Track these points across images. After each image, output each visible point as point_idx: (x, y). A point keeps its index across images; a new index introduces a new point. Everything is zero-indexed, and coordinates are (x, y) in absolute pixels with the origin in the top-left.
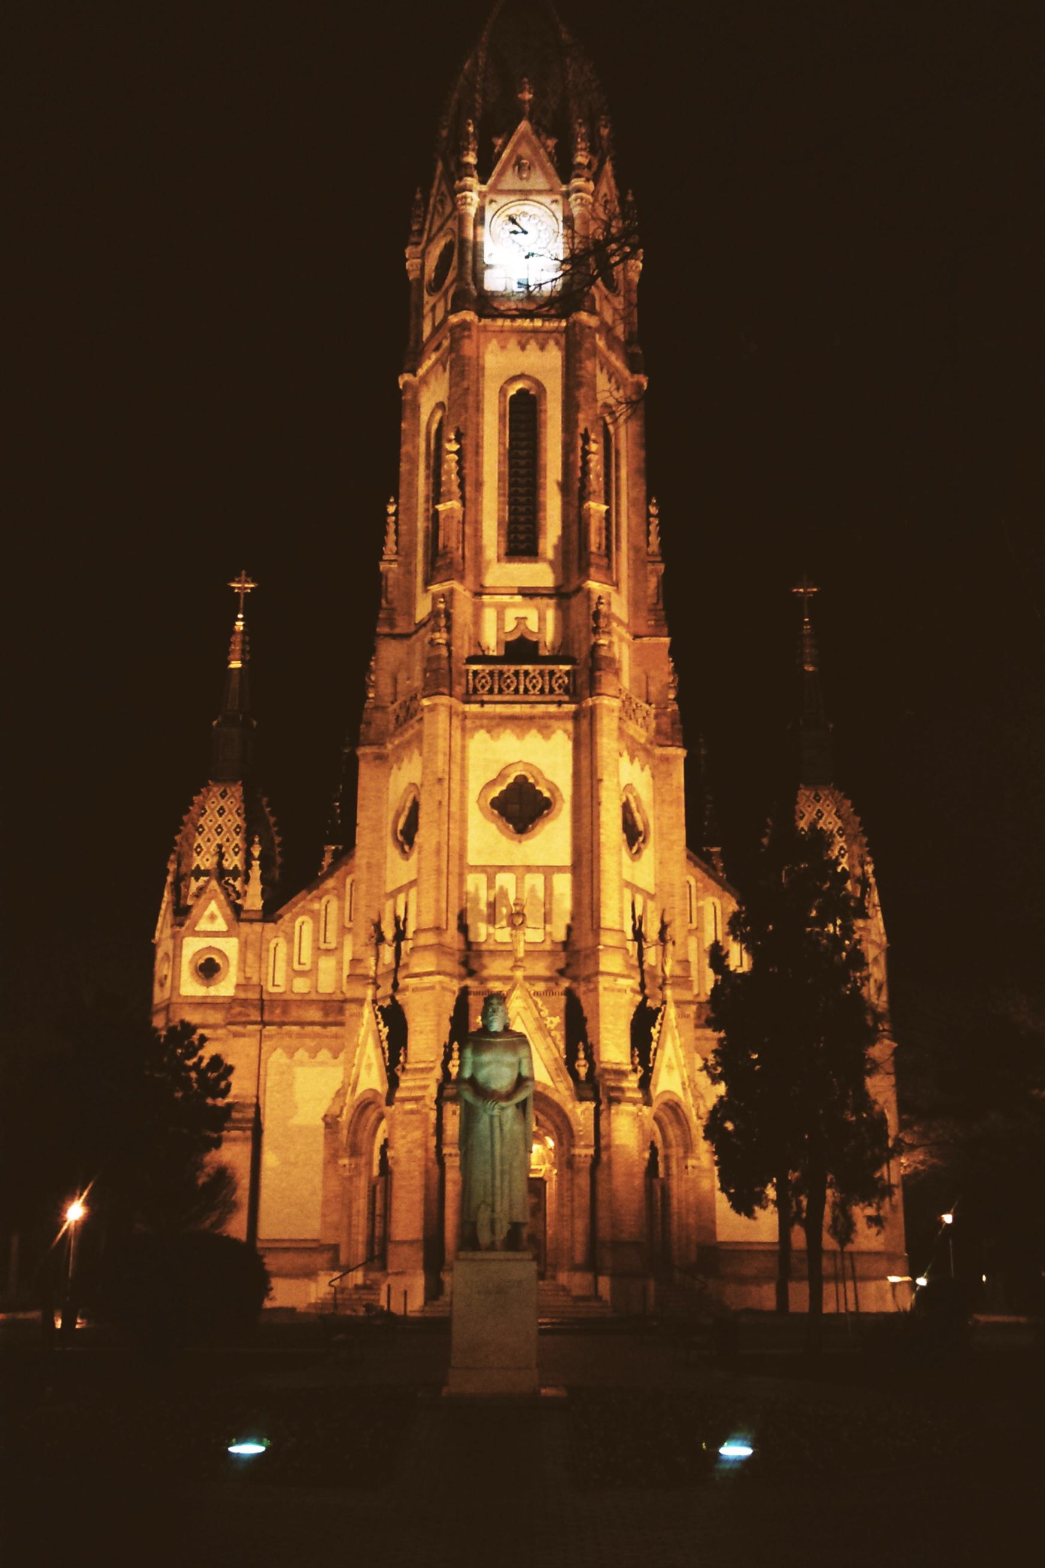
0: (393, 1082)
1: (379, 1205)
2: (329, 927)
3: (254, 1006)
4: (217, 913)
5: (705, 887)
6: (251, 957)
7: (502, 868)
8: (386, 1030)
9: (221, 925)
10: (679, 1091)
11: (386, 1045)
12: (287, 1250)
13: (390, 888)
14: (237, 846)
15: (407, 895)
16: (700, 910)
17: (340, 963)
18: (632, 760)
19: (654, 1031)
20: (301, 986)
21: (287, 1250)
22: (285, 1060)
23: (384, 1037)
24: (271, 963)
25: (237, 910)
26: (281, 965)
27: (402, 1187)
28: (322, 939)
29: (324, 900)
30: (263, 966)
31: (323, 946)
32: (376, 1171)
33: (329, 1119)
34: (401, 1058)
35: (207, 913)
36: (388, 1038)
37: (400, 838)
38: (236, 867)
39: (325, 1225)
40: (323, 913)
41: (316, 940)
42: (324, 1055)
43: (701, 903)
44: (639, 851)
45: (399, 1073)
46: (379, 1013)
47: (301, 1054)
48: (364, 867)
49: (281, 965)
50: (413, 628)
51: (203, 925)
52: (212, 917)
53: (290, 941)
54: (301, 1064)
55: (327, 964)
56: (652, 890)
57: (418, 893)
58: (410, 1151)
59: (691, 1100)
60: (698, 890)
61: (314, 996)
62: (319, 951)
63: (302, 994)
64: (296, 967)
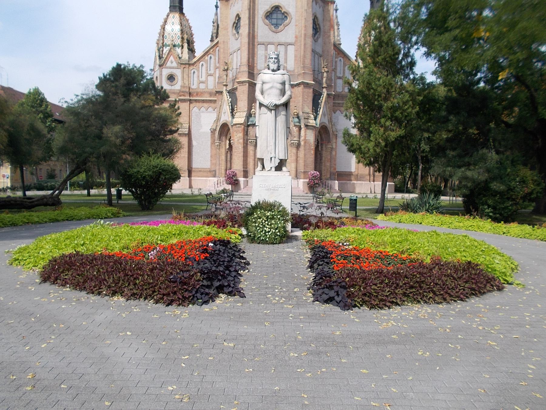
0: (233, 116)
1: (228, 157)
2: (211, 65)
4: (173, 60)
5: (338, 54)
6: (186, 76)
7: (270, 43)
8: (230, 99)
9: (174, 64)
10: (327, 123)
11: (230, 104)
12: (200, 171)
13: (231, 51)
14: (179, 36)
15: (237, 54)
16: (336, 62)
17: (215, 78)
18: (316, 4)
19: (319, 101)
20: (202, 86)
21: (200, 171)
22: (197, 111)
23: (229, 102)
24: (192, 78)
26: (196, 79)
27: (235, 152)
28: (209, 70)
29: (209, 56)
30: (190, 79)
31: (209, 72)
32: (228, 147)
33: (212, 130)
36: (231, 102)
37: (234, 32)
38: (179, 44)
39: (212, 164)
40: (209, 60)
41: (207, 70)
42: (210, 109)
43: (336, 60)
44: (318, 38)
46: (228, 94)
47: (203, 109)
48: (222, 43)
49: (196, 79)
51: (169, 64)
52: (172, 62)
53: (198, 71)
54: (203, 112)
55: (211, 79)
56: (321, 53)
57: (241, 53)
58: (238, 140)
59: (330, 126)
60: (336, 55)
61: (206, 90)
63: (203, 89)
64: (201, 79)
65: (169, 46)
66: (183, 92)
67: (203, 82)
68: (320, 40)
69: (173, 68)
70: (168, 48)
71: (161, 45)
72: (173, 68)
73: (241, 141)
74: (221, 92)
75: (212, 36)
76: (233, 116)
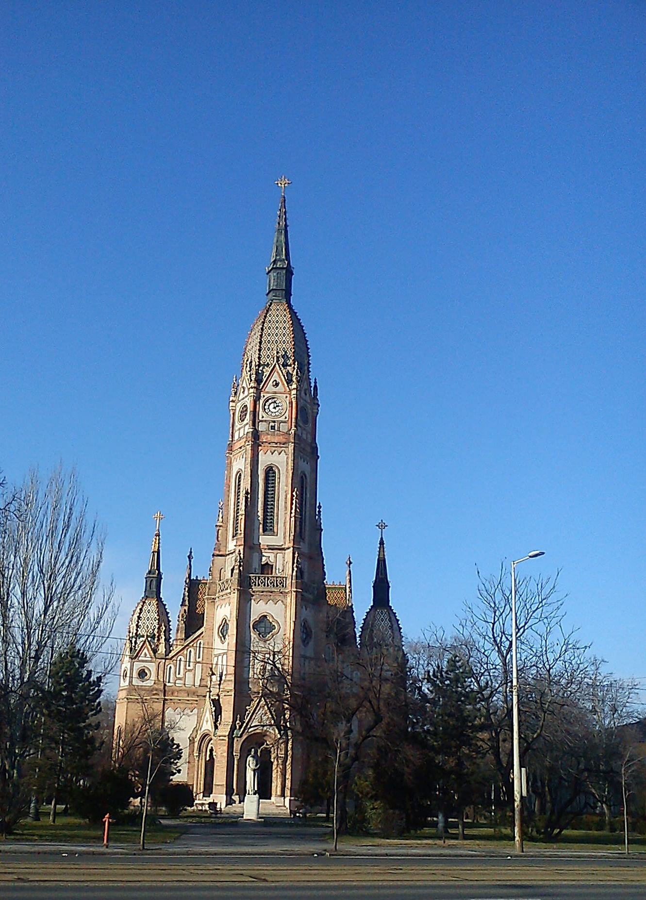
0: (216, 727)
3: (161, 691)
8: (214, 708)
11: (214, 713)
23: (213, 711)
25: (155, 651)
34: (219, 719)
35: (143, 653)
45: (218, 725)
50: (227, 553)
55: (189, 675)
62: (187, 671)
64: (178, 676)
65: (143, 636)
66: (156, 690)
67: (180, 679)
68: (311, 644)
69: (146, 661)
70: (142, 639)
71: (134, 635)
72: (146, 661)
73: (225, 754)
74: (205, 696)
75: (183, 599)
76: (216, 727)
